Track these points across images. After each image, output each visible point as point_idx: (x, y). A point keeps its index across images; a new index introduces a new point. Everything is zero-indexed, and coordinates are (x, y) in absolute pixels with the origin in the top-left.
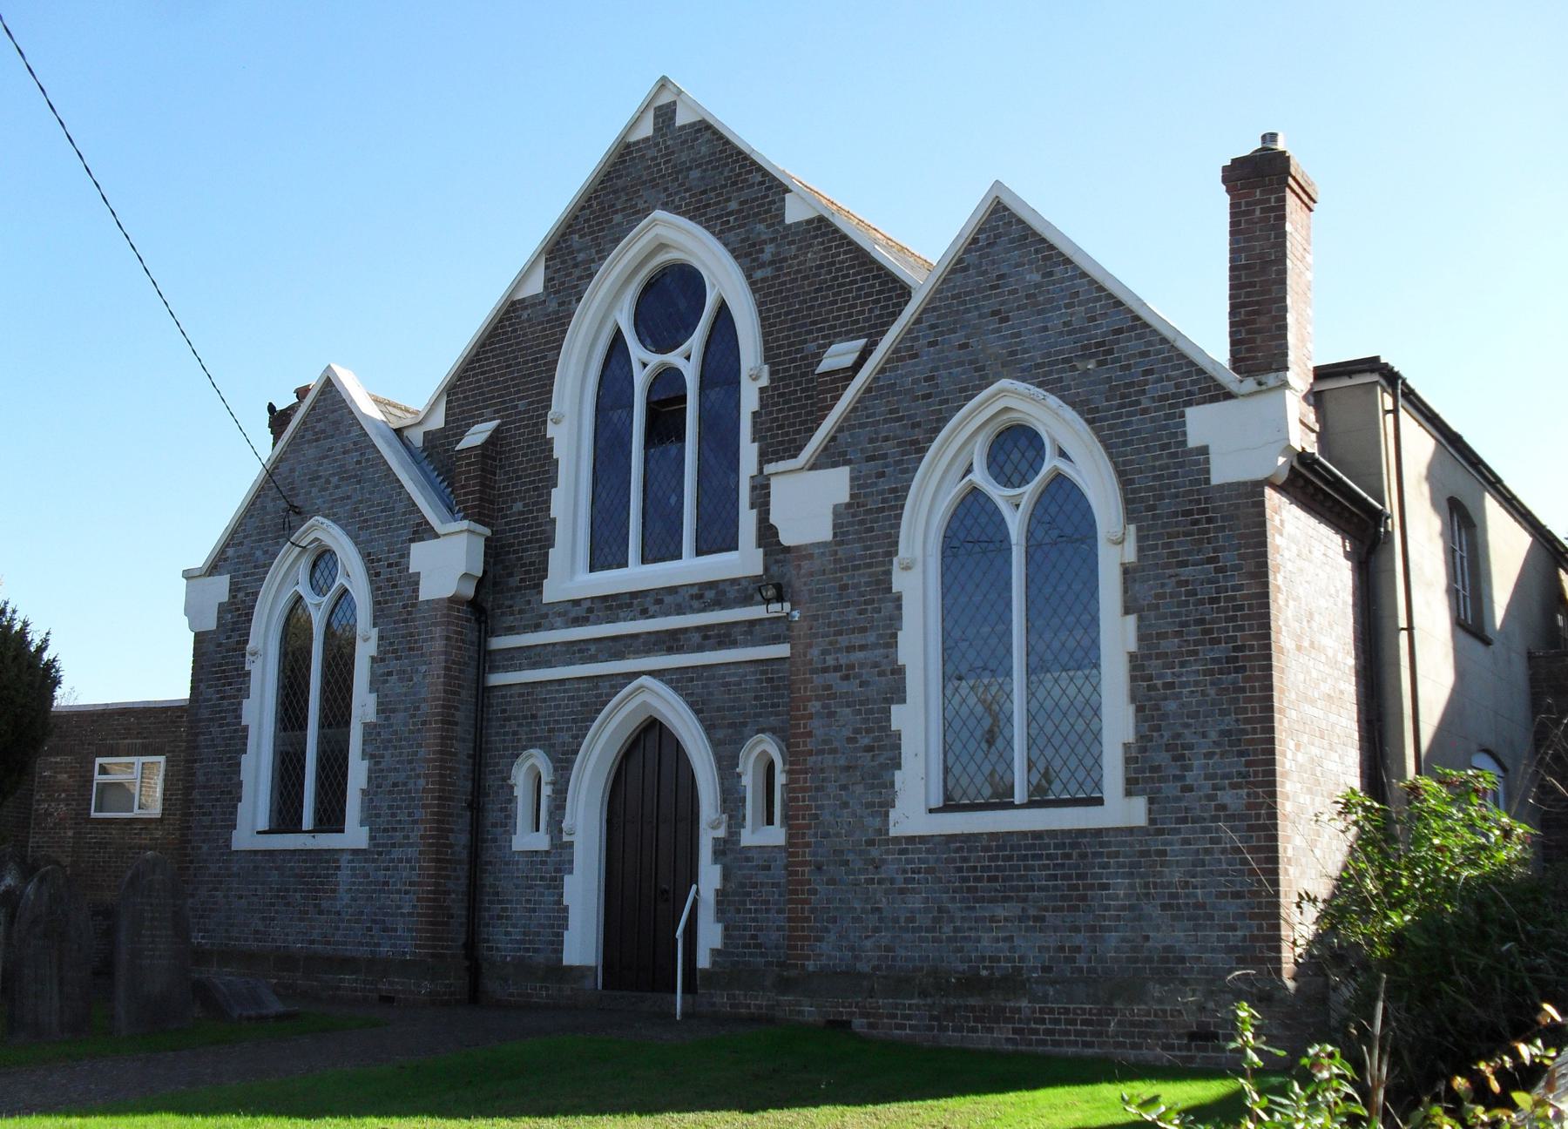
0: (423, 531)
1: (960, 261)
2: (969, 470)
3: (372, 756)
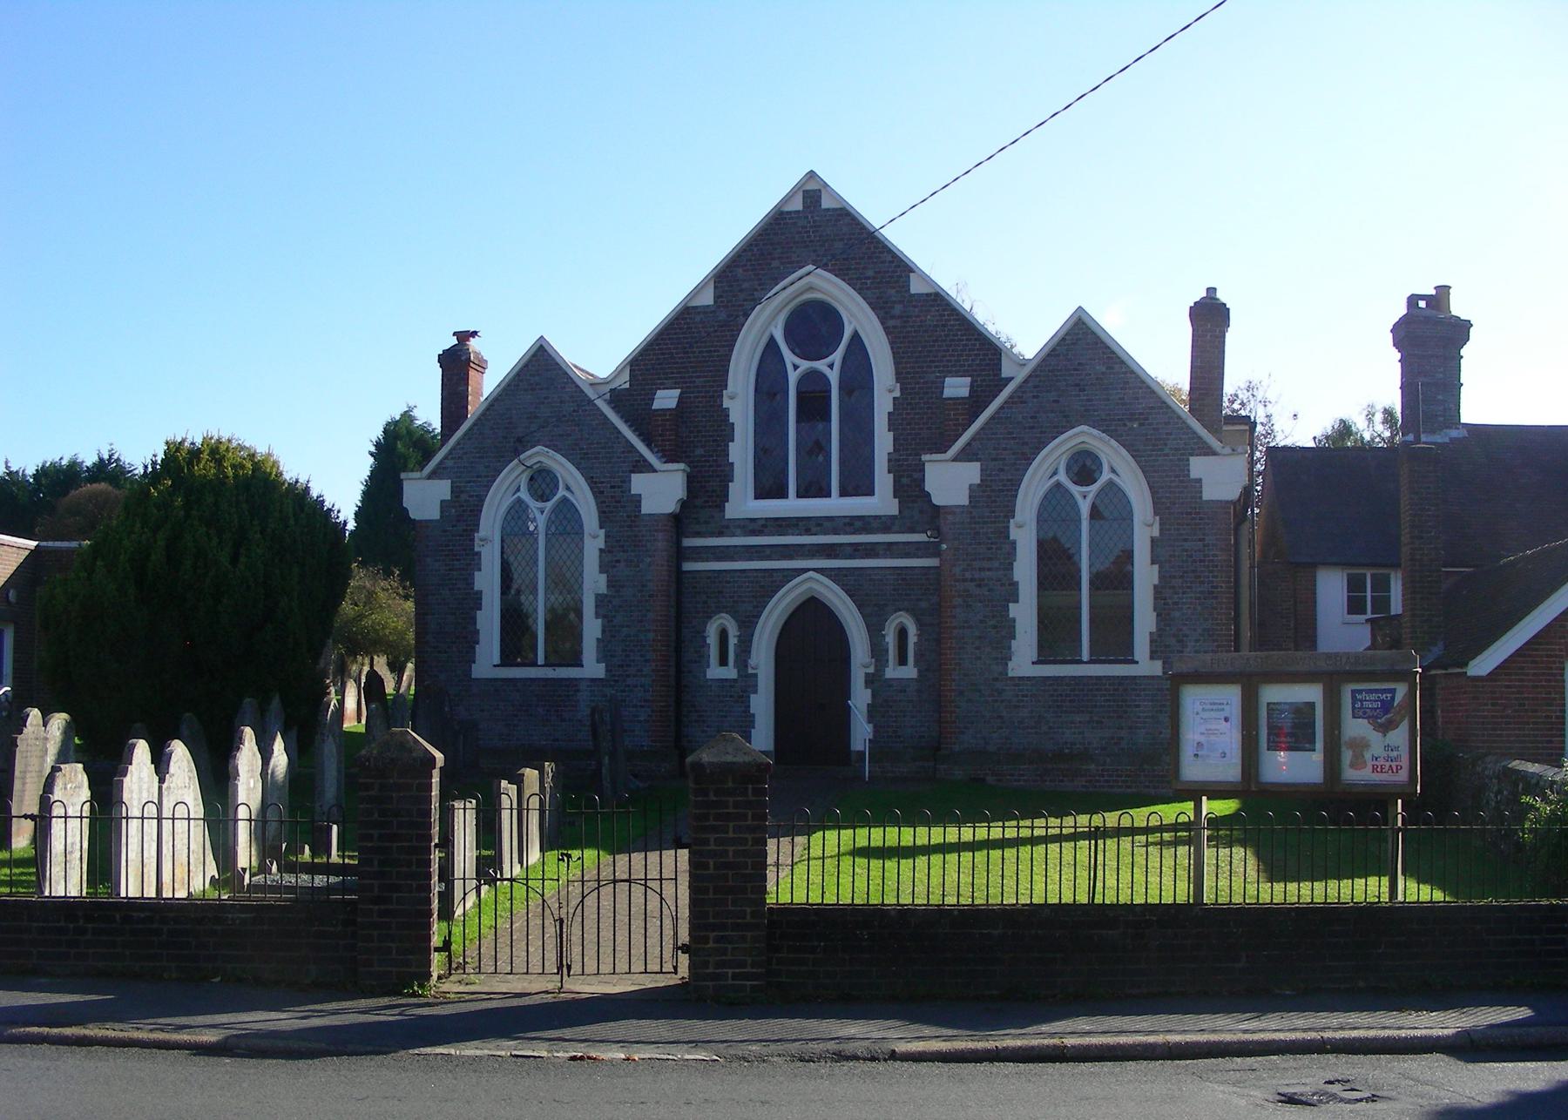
0: (643, 466)
1: (1054, 350)
2: (1055, 473)
3: (604, 617)
